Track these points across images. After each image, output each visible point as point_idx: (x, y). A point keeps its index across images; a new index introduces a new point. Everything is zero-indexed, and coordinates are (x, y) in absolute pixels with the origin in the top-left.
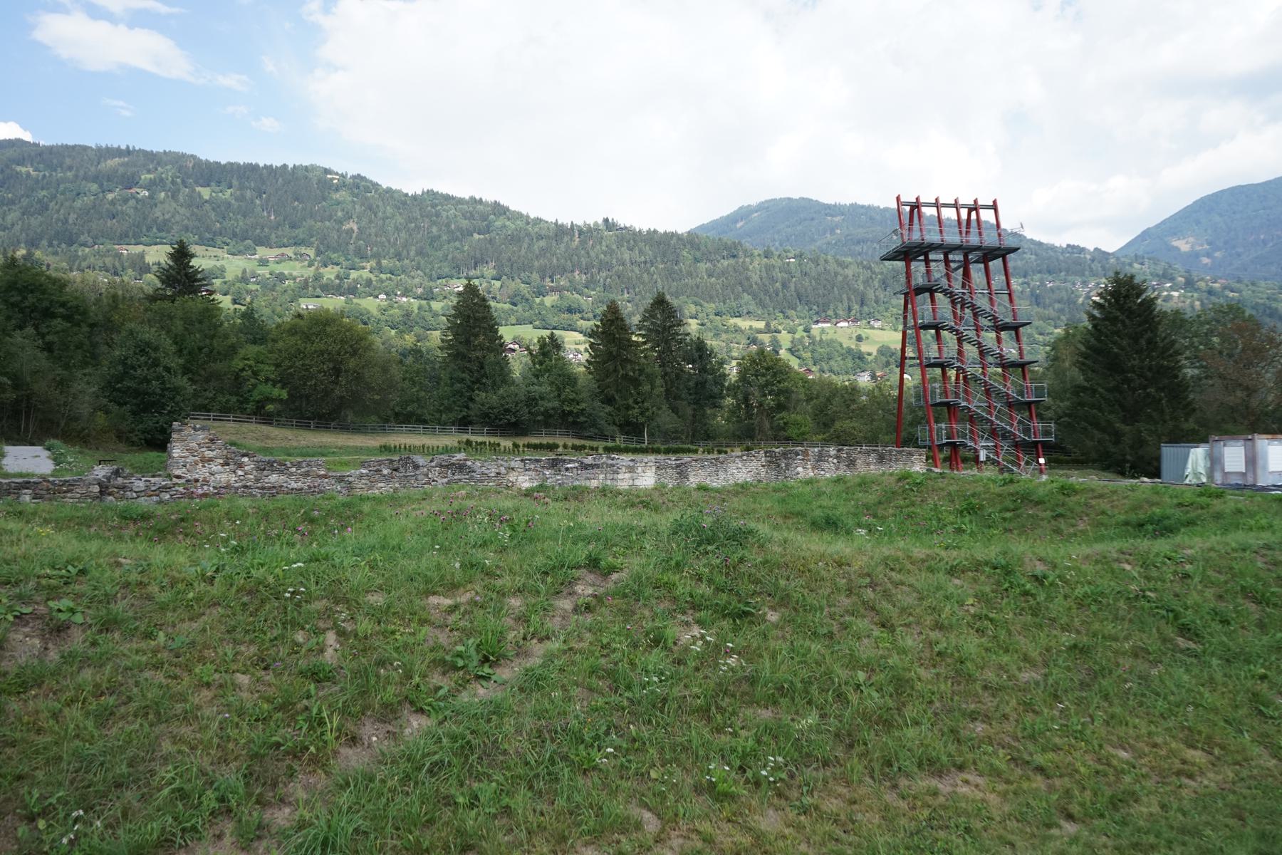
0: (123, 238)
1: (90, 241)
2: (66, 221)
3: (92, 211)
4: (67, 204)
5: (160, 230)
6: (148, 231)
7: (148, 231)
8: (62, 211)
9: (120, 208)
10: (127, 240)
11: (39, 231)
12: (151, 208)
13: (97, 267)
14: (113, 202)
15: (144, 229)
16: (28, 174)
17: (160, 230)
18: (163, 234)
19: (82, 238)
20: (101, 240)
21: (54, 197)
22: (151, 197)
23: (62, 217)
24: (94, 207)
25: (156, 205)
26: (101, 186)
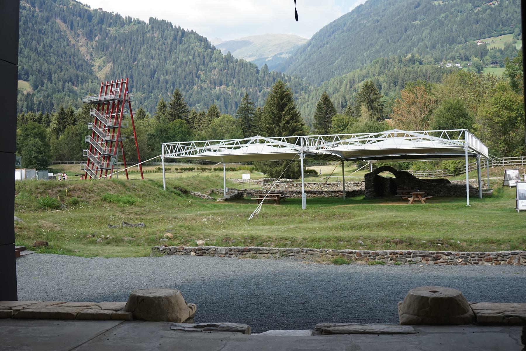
0: (481, 35)
1: (463, 39)
2: (451, 31)
3: (465, 22)
4: (452, 20)
5: (504, 26)
6: (497, 27)
7: (497, 27)
8: (449, 25)
9: (481, 16)
10: (483, 35)
11: (436, 39)
12: (500, 12)
13: (456, 57)
14: (477, 14)
15: (494, 27)
16: (439, 5)
17: (504, 26)
18: (507, 28)
19: (459, 39)
20: (470, 38)
21: (447, 16)
22: (500, 5)
23: (449, 28)
24: (467, 19)
25: (502, 10)
26: (473, 4)
